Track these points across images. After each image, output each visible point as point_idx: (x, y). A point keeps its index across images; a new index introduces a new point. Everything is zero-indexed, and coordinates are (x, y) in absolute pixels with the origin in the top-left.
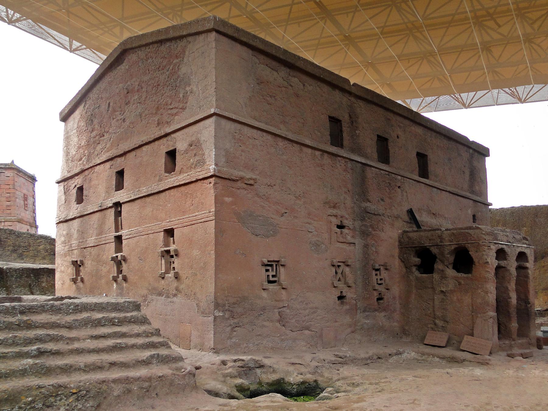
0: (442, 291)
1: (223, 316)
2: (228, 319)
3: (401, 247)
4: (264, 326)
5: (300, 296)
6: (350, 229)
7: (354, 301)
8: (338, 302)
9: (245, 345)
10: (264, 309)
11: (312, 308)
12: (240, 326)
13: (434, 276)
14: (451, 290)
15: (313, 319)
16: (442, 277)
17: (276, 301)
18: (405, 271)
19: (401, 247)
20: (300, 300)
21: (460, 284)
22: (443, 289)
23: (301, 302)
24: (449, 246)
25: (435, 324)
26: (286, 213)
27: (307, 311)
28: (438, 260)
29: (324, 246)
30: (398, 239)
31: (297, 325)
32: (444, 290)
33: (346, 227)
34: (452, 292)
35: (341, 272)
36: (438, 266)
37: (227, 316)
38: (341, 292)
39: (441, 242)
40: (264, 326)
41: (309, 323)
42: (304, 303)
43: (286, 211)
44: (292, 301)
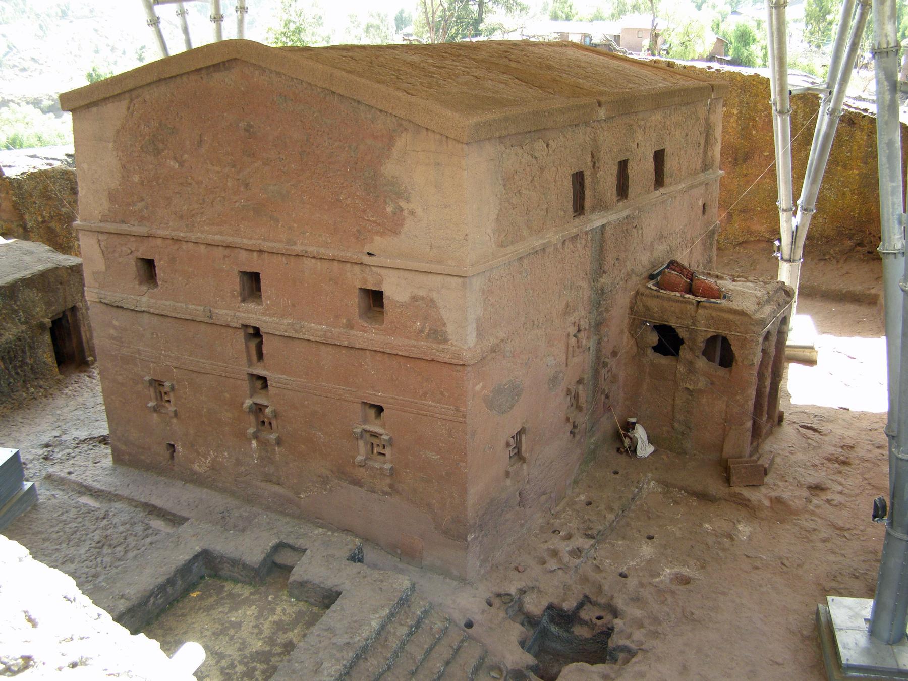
0: (688, 389)
3: (633, 317)
13: (679, 367)
14: (700, 390)
16: (689, 370)
18: (636, 351)
19: (633, 317)
21: (713, 383)
22: (689, 387)
24: (705, 331)
25: (673, 428)
28: (686, 347)
30: (628, 305)
32: (691, 388)
34: (701, 392)
36: (684, 352)
39: (694, 324)
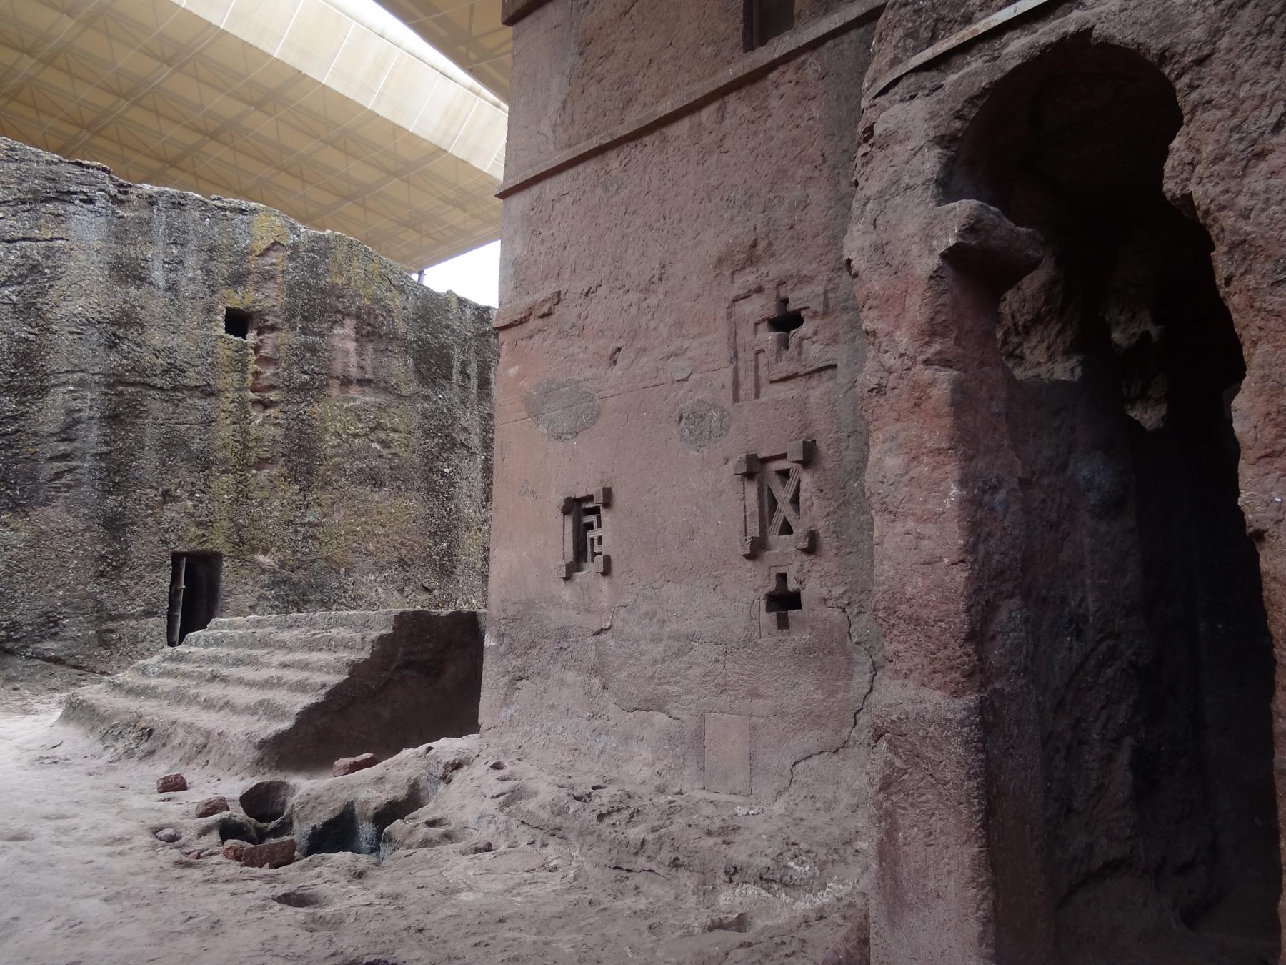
1: (497, 648)
2: (505, 655)
4: (562, 683)
5: (645, 597)
6: (815, 315)
7: (836, 613)
8: (768, 619)
9: (526, 728)
10: (563, 634)
11: (674, 637)
12: (527, 678)
15: (677, 673)
17: (587, 610)
20: (643, 611)
23: (646, 614)
26: (619, 349)
27: (662, 647)
29: (716, 415)
31: (632, 689)
33: (803, 313)
35: (789, 496)
37: (502, 649)
38: (783, 578)
40: (562, 683)
41: (666, 687)
42: (656, 619)
43: (619, 345)
44: (622, 611)
